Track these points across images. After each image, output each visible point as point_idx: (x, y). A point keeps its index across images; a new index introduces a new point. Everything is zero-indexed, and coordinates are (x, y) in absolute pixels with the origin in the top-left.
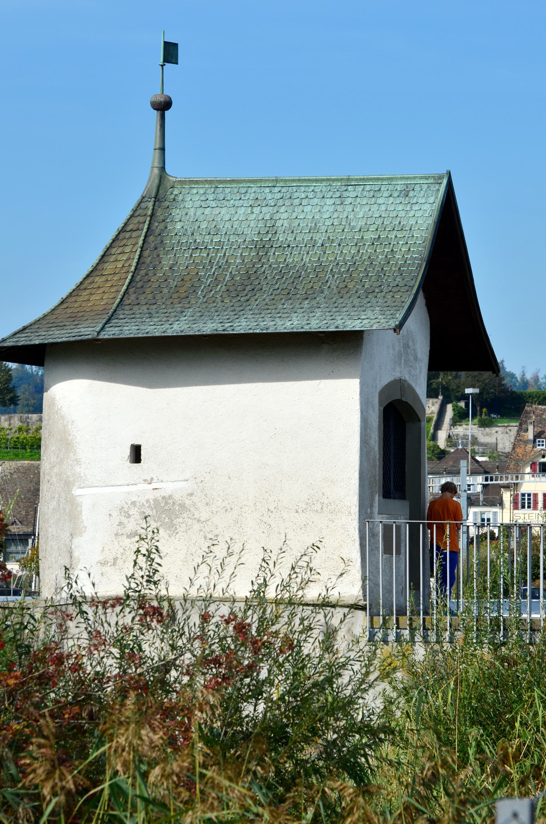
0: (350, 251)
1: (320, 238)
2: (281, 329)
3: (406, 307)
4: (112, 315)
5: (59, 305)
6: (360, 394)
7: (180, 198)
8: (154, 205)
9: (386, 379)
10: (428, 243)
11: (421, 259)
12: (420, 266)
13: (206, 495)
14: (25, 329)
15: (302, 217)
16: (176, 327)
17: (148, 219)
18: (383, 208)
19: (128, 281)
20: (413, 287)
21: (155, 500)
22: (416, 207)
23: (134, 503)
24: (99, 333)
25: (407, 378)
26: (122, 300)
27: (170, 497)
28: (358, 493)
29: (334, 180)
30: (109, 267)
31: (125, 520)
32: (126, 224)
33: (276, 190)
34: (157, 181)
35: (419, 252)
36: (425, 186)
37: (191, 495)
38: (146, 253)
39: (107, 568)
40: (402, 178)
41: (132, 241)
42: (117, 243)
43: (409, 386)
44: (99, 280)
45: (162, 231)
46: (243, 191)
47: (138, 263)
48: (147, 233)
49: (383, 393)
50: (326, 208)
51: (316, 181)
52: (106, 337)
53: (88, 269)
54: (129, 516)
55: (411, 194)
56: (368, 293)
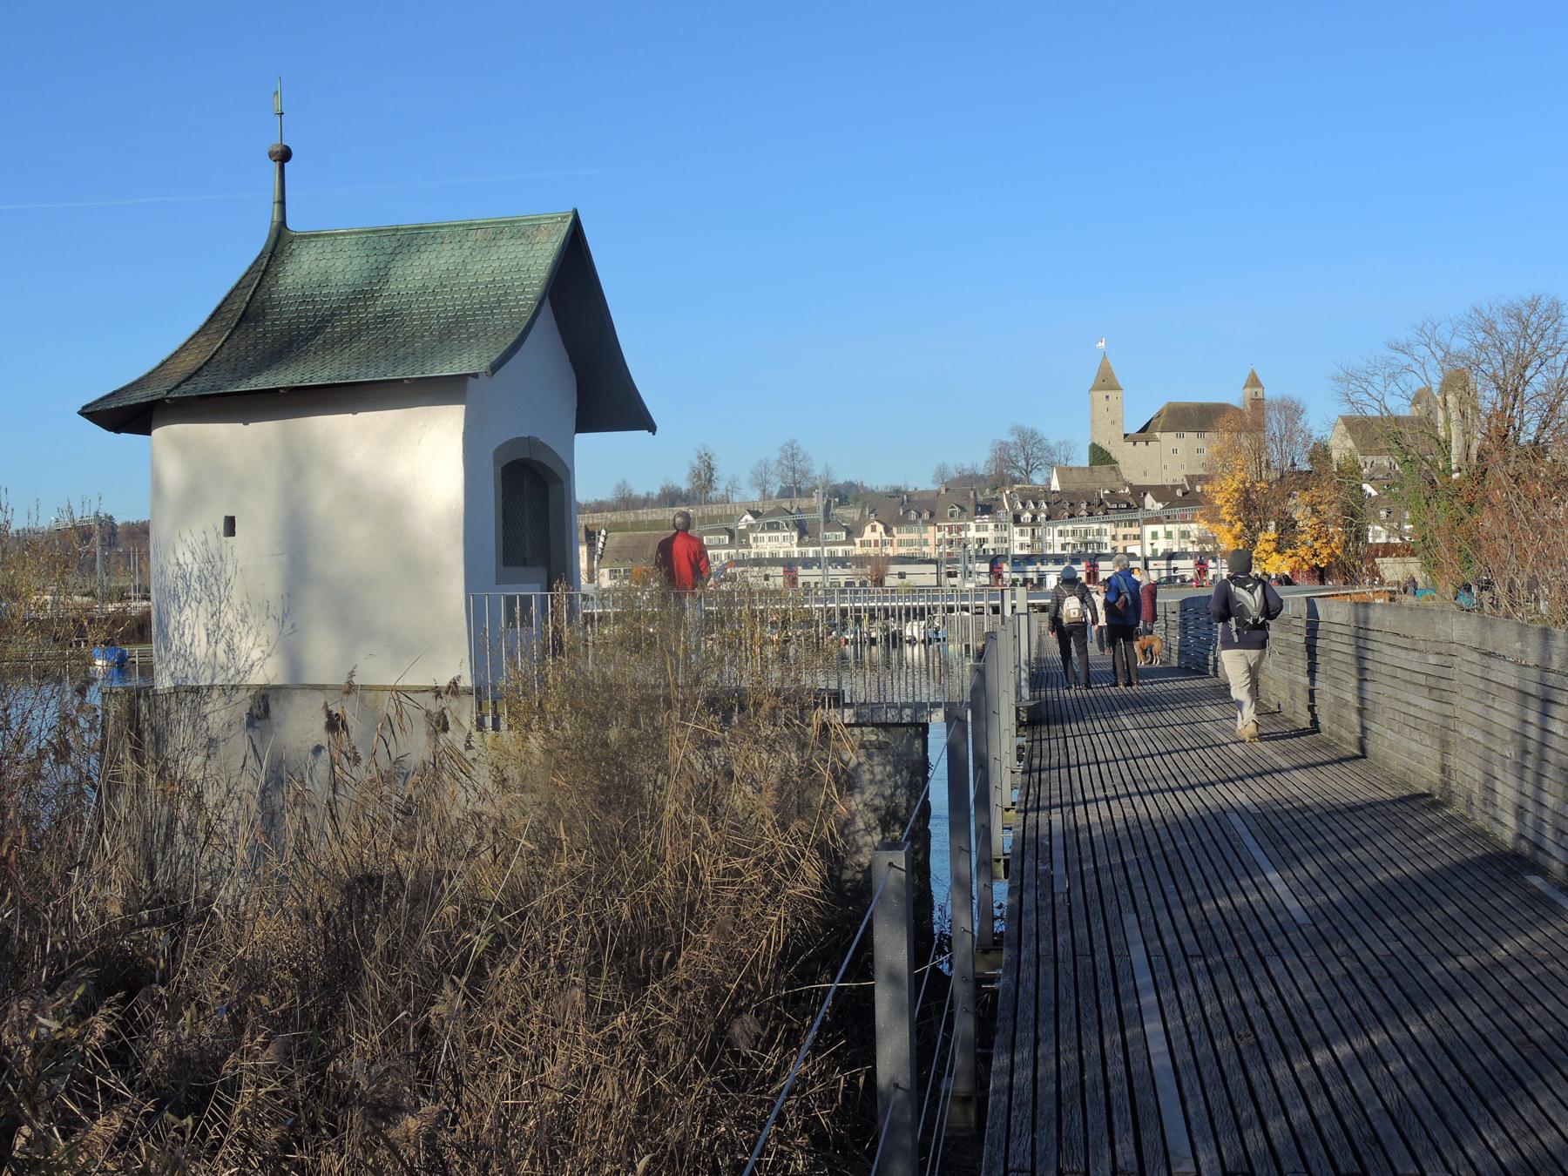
5: (158, 367)
6: (464, 451)
7: (298, 250)
8: (269, 261)
14: (113, 394)
15: (417, 263)
17: (261, 274)
19: (224, 337)
20: (518, 329)
24: (169, 392)
26: (212, 358)
29: (455, 226)
32: (240, 282)
34: (275, 236)
41: (241, 298)
42: (228, 302)
44: (202, 339)
45: (273, 286)
48: (256, 289)
52: (176, 395)
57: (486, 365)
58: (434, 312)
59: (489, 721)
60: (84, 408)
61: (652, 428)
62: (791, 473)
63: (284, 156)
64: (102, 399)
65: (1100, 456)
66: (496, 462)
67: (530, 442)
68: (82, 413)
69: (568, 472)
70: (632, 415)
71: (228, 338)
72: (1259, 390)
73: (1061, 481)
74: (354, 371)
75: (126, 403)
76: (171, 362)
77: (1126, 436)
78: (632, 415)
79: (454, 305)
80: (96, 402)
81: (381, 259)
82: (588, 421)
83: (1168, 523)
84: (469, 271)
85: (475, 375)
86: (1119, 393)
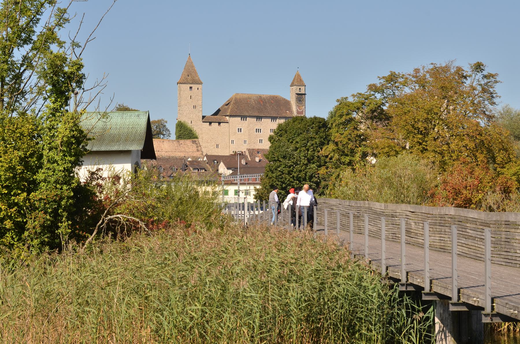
0: (126, 130)
1: (118, 127)
2: (113, 150)
10: (146, 128)
22: (141, 120)
56: (133, 140)
72: (303, 88)
77: (203, 117)
83: (241, 184)
86: (200, 86)
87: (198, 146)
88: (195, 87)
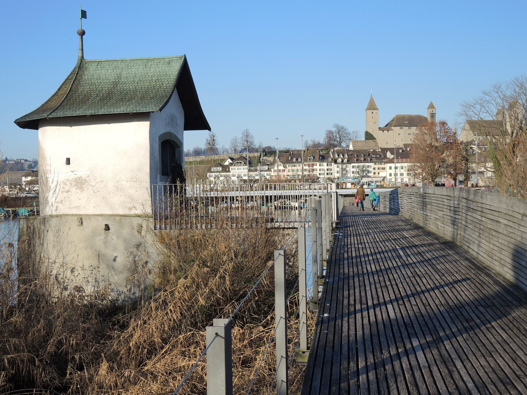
1: (136, 80)
3: (164, 103)
4: (56, 109)
6: (150, 137)
9: (162, 131)
11: (173, 86)
12: (172, 88)
13: (94, 176)
14: (26, 115)
16: (77, 112)
18: (160, 69)
21: (75, 179)
22: (172, 68)
23: (68, 180)
24: (48, 115)
25: (173, 132)
26: (61, 104)
27: (81, 177)
28: (149, 173)
30: (60, 92)
31: (65, 186)
32: (68, 77)
33: (123, 63)
34: (80, 61)
35: (172, 84)
36: (176, 60)
37: (88, 176)
38: (73, 87)
39: (59, 204)
40: (168, 58)
41: (69, 83)
42: (65, 84)
43: (174, 135)
44: (56, 97)
45: (80, 79)
46: (111, 64)
47: (70, 91)
49: (160, 137)
50: (140, 69)
51: (137, 60)
53: (53, 93)
54: (66, 185)
55: (171, 63)
57: (158, 109)
58: (138, 90)
59: (158, 226)
60: (17, 120)
61: (209, 129)
62: (246, 143)
63: (82, 34)
64: (22, 117)
65: (369, 136)
66: (159, 140)
67: (170, 134)
68: (15, 122)
69: (182, 144)
70: (204, 125)
71: (66, 97)
72: (434, 110)
73: (354, 147)
74: (112, 110)
75: (32, 119)
76: (46, 105)
77: (379, 128)
78: (204, 125)
79: (145, 88)
80: (20, 118)
81: (118, 71)
82: (189, 126)
84: (149, 76)
85: (153, 112)
87: (377, 143)
88: (374, 111)
